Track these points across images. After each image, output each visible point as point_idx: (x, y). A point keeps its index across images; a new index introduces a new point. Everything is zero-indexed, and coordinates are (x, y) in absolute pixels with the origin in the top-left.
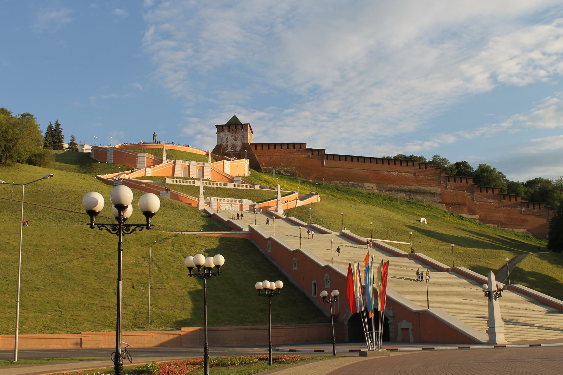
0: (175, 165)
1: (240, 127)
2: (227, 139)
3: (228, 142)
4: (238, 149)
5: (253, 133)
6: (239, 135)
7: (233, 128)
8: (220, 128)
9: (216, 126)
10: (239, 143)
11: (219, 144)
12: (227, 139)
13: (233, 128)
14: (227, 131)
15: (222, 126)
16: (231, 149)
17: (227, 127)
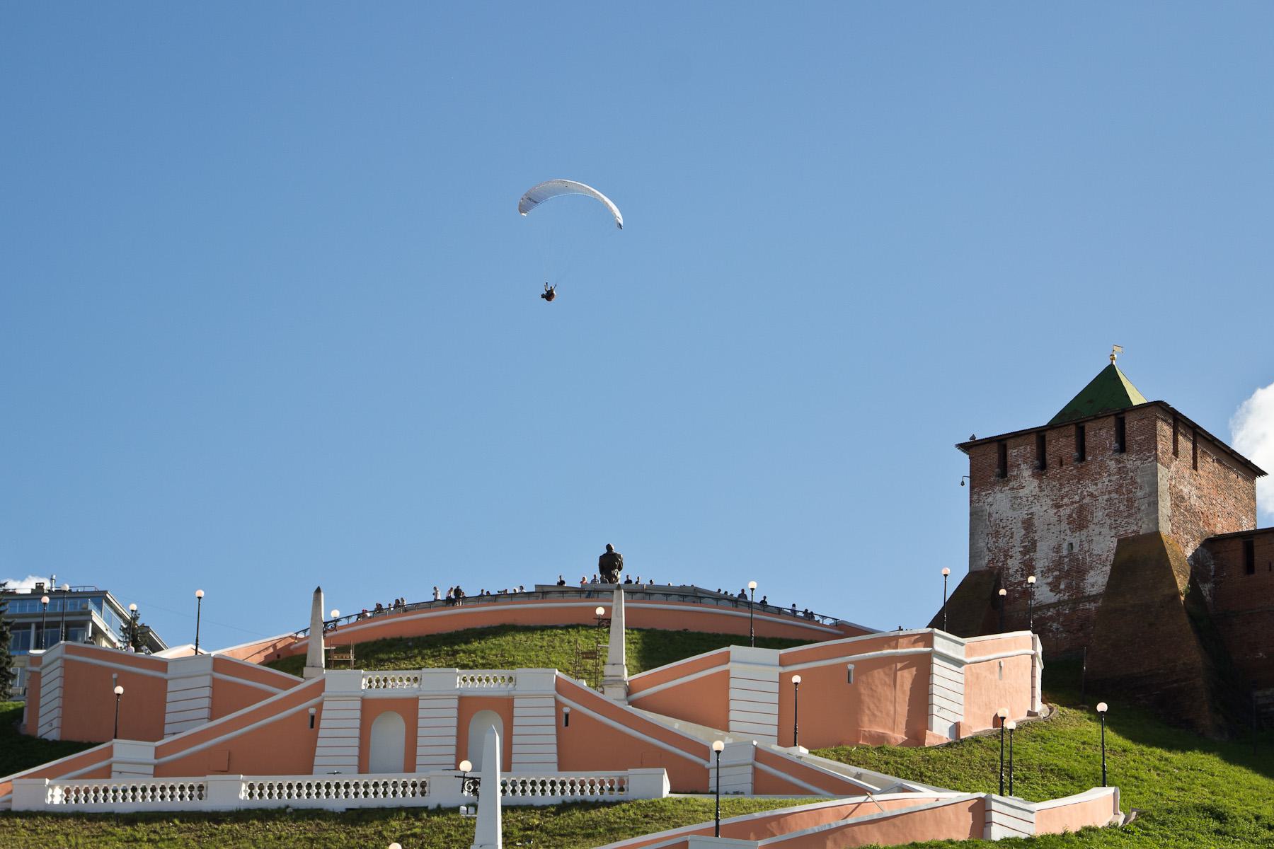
0: (319, 707)
1: (1101, 434)
2: (1028, 524)
3: (1030, 548)
4: (1096, 581)
5: (1252, 471)
6: (1099, 487)
7: (1062, 446)
8: (991, 459)
9: (964, 447)
10: (1103, 544)
11: (983, 563)
12: (1028, 524)
13: (1062, 446)
14: (1026, 473)
15: (1001, 442)
16: (1054, 587)
17: (1029, 449)
